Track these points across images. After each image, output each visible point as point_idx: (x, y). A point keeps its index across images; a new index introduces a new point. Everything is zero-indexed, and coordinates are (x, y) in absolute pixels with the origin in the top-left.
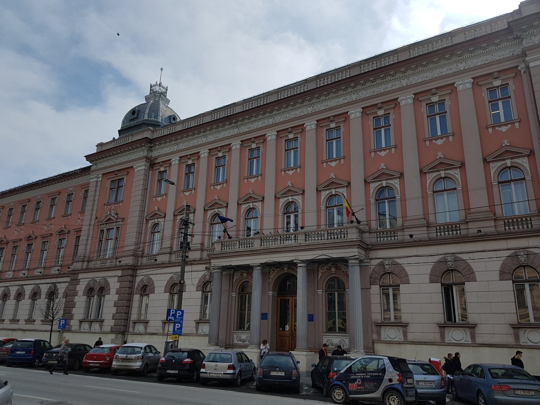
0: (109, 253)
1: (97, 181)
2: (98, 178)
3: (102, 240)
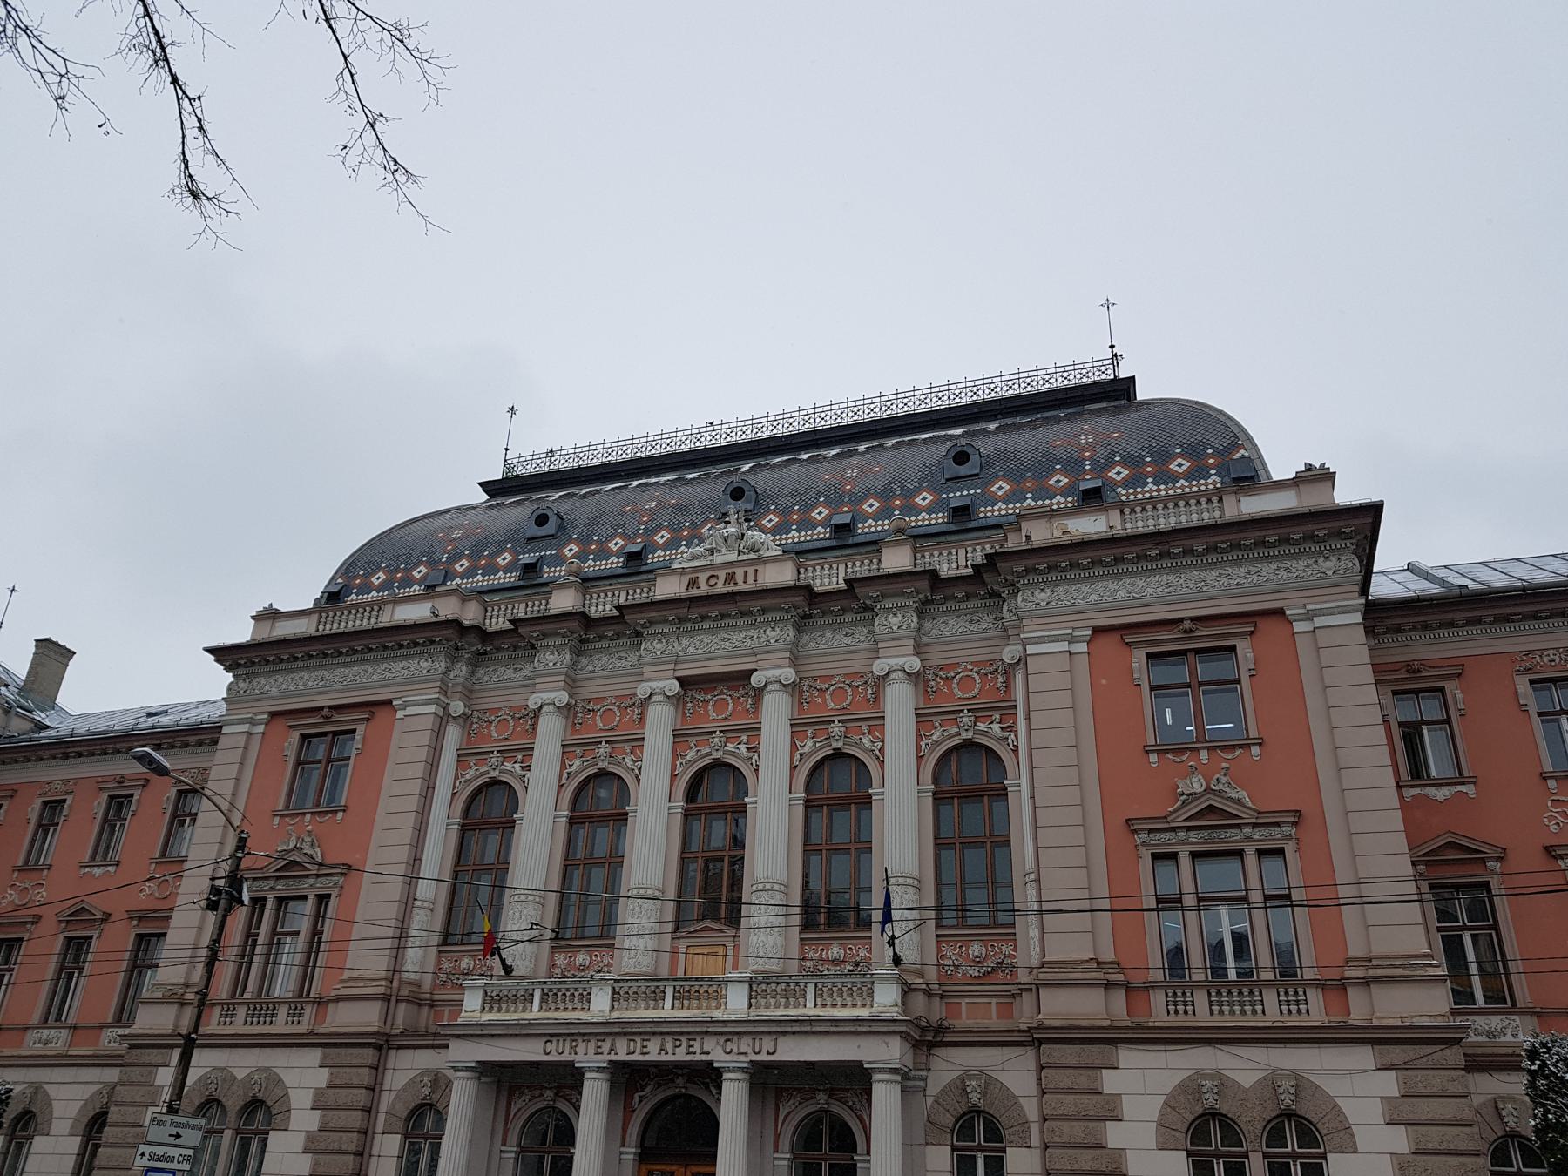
3: (258, 935)
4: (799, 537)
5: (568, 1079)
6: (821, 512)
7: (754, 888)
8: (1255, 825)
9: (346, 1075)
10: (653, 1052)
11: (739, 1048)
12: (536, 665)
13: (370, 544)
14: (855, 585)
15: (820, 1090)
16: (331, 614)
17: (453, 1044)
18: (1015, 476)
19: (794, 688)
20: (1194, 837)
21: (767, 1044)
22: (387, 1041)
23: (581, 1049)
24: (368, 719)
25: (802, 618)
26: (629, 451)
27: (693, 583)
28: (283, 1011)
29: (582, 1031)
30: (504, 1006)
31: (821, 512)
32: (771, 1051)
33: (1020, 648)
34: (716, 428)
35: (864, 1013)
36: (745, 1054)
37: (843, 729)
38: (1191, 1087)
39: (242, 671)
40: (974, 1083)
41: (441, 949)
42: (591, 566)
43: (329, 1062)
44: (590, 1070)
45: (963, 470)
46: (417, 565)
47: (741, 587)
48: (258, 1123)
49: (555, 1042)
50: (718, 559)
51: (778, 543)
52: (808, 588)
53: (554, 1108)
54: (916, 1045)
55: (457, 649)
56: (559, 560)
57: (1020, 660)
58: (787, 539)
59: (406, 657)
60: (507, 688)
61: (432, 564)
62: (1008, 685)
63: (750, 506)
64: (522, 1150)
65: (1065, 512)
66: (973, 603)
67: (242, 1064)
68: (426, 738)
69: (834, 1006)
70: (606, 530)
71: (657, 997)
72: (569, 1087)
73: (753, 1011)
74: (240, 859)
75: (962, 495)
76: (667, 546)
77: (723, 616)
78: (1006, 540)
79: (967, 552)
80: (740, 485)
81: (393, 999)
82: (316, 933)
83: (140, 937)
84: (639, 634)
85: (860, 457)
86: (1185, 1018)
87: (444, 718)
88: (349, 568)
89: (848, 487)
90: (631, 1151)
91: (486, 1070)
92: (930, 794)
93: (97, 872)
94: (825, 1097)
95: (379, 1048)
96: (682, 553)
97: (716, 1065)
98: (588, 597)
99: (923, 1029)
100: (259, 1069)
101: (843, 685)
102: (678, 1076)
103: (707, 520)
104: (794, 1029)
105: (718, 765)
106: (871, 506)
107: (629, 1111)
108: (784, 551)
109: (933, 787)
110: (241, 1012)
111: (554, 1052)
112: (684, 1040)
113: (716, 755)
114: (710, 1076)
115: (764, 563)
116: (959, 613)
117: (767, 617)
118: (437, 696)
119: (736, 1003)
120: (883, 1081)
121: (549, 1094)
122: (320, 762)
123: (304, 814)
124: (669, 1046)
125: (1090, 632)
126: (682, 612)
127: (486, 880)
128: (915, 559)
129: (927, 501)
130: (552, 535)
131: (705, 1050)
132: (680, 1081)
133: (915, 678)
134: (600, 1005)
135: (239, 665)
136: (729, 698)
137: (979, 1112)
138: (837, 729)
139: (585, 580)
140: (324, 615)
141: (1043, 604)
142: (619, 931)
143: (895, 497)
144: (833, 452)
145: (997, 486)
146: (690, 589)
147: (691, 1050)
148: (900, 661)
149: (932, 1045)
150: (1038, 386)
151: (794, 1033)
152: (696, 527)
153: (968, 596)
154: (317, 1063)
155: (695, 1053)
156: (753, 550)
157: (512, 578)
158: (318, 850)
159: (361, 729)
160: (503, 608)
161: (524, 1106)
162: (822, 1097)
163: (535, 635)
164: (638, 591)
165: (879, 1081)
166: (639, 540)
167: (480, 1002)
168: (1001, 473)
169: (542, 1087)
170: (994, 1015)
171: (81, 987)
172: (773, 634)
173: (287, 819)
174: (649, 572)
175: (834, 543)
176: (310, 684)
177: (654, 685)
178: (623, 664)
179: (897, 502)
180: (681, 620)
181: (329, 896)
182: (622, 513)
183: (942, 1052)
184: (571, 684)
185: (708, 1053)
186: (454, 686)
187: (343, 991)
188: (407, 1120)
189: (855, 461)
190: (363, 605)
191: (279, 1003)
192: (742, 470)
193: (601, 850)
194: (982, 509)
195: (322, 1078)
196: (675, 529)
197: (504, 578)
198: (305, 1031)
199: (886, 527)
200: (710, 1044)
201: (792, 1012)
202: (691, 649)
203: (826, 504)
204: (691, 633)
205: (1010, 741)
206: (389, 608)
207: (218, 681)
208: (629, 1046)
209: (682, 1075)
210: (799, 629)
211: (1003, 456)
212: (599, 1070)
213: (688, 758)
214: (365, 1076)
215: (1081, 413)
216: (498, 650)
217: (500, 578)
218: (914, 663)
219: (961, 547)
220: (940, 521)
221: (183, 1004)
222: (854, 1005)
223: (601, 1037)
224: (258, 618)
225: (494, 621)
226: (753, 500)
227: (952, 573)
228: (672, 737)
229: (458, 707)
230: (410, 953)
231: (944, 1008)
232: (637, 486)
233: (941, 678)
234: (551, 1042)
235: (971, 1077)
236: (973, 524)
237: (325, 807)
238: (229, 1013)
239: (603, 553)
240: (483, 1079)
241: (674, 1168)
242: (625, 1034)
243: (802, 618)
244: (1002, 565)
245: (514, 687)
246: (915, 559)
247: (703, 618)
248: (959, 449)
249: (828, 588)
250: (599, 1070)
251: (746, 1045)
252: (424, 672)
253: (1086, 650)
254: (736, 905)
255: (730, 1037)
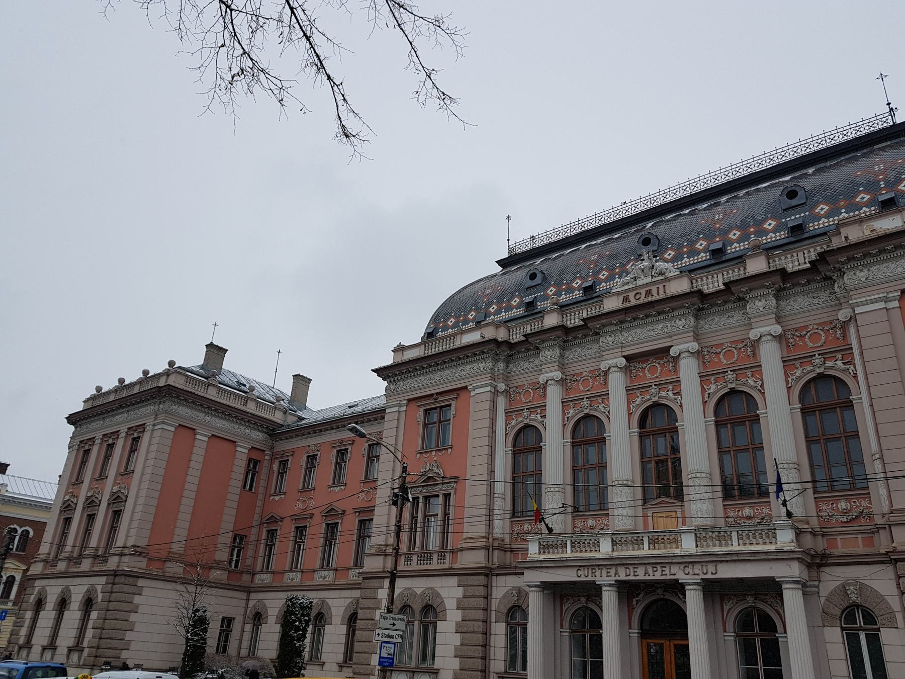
0: (434, 542)
1: (399, 412)
2: (400, 406)
4: (690, 261)
5: (593, 591)
6: (701, 245)
7: (690, 476)
9: (471, 591)
10: (641, 575)
11: (693, 571)
12: (541, 358)
13: (445, 304)
14: (730, 286)
15: (748, 595)
16: (430, 344)
17: (526, 572)
18: (832, 200)
19: (698, 354)
21: (711, 568)
22: (491, 572)
23: (598, 573)
24: (456, 398)
25: (698, 311)
26: (577, 228)
27: (626, 299)
28: (435, 557)
29: (597, 564)
30: (551, 551)
31: (701, 245)
32: (714, 572)
33: (851, 310)
34: (628, 205)
35: (772, 548)
36: (698, 574)
37: (734, 376)
39: (391, 379)
40: (852, 588)
41: (512, 520)
42: (564, 298)
43: (462, 583)
44: (605, 585)
45: (794, 202)
46: (470, 312)
47: (656, 297)
48: (431, 617)
49: (582, 570)
50: (639, 282)
51: (676, 267)
52: (700, 292)
53: (587, 608)
54: (809, 566)
55: (497, 355)
56: (546, 297)
57: (851, 318)
58: (681, 264)
59: (472, 362)
60: (526, 373)
61: (477, 310)
62: (845, 336)
63: (655, 248)
64: (572, 631)
65: (871, 218)
66: (813, 286)
67: (419, 586)
68: (487, 405)
69: (751, 544)
70: (569, 277)
71: (638, 543)
72: (593, 596)
73: (700, 550)
74: (405, 477)
75: (796, 218)
76: (607, 280)
77: (647, 316)
78: (831, 241)
79: (804, 254)
80: (647, 236)
81: (491, 548)
82: (446, 514)
83: (361, 522)
84: (597, 334)
85: (722, 206)
87: (495, 393)
88: (436, 318)
89: (718, 226)
90: (635, 632)
91: (545, 586)
92: (799, 410)
93: (336, 489)
94: (753, 599)
95: (487, 575)
96: (617, 282)
97: (680, 581)
98: (565, 316)
99: (813, 556)
100: (427, 588)
101: (730, 349)
102: (658, 588)
103: (630, 261)
104: (727, 559)
105: (656, 405)
106: (735, 235)
107: (631, 609)
108: (681, 272)
109: (800, 405)
110: (415, 558)
111: (583, 576)
112: (659, 567)
113: (654, 399)
114: (678, 588)
115: (669, 281)
116: (804, 293)
117: (676, 313)
118: (490, 381)
119: (688, 545)
120: (790, 589)
121: (583, 599)
122: (435, 423)
123: (432, 451)
124: (650, 571)
125: (899, 294)
126: (622, 317)
127: (531, 481)
128: (769, 263)
129: (772, 226)
130: (540, 284)
131: (673, 573)
132: (659, 591)
133: (779, 338)
134: (605, 548)
135: (389, 377)
136: (657, 365)
137: (858, 606)
138: (730, 376)
139: (561, 307)
140: (427, 345)
141: (863, 279)
142: (610, 506)
143: (749, 227)
144: (705, 206)
145: (819, 208)
146: (625, 303)
147: (664, 573)
148: (768, 329)
149: (820, 566)
150: (839, 139)
151: (727, 561)
152: (623, 266)
153: (809, 282)
154: (456, 584)
155: (666, 575)
156: (661, 274)
157: (521, 312)
158: (441, 470)
159: (453, 403)
160: (518, 329)
161: (570, 607)
162: (750, 599)
163: (538, 341)
164: (593, 308)
165: (787, 589)
166: (590, 279)
167: (537, 548)
168: (820, 200)
169: (579, 596)
170: (861, 545)
171: (336, 549)
172: (680, 323)
173: (424, 455)
174: (599, 296)
175: (713, 261)
176: (425, 382)
177: (610, 362)
178: (590, 352)
179: (752, 230)
180: (621, 322)
181: (450, 494)
182: (578, 265)
183: (827, 569)
184: (562, 367)
185: (674, 575)
186: (498, 375)
187: (464, 545)
188: (507, 615)
189: (720, 208)
190: (446, 337)
191: (433, 553)
192: (648, 227)
193: (593, 459)
194: (811, 225)
195: (459, 593)
196: (611, 269)
197: (517, 312)
198: (447, 568)
199: (747, 246)
200: (675, 569)
201: (725, 549)
202: (630, 339)
203: (704, 239)
204: (629, 329)
205: (850, 371)
206: (459, 336)
207: (379, 386)
208: (626, 571)
209: (660, 588)
210: (697, 317)
211: (821, 188)
212: (610, 585)
213: (637, 402)
214: (482, 591)
215: (874, 150)
216: (519, 352)
217: (514, 312)
218: (777, 329)
219: (800, 251)
220: (783, 237)
221: (386, 555)
222: (765, 543)
223: (609, 567)
224: (395, 351)
225: (514, 336)
226: (657, 244)
227: (796, 269)
228: (625, 392)
229: (502, 386)
230: (496, 523)
231: (825, 542)
232: (585, 248)
233: (797, 336)
234: (580, 570)
235: (849, 584)
236: (806, 235)
237: (442, 446)
238: (409, 560)
239: (570, 290)
240: (545, 592)
241: (662, 641)
242: (623, 565)
243: (698, 311)
244: (832, 258)
245: (530, 372)
246: (769, 263)
247: (635, 319)
248: (790, 189)
249: (713, 290)
250: (610, 585)
251: (697, 569)
252: (482, 369)
253: (898, 305)
255: (687, 565)
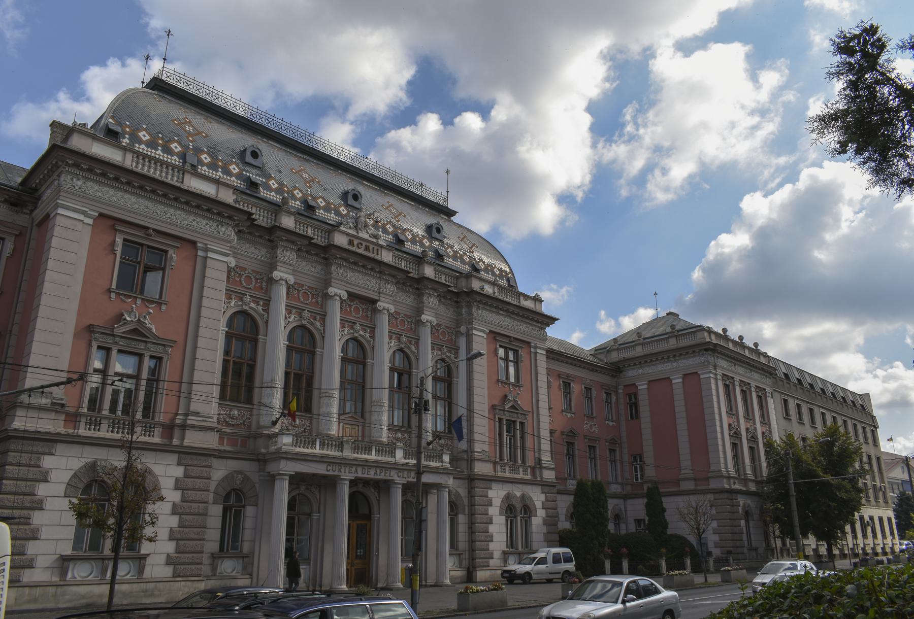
8: (154, 343)
20: (122, 342)
38: (92, 467)
86: (94, 432)
111: (331, 471)
125: (97, 214)
254: (250, 389)
